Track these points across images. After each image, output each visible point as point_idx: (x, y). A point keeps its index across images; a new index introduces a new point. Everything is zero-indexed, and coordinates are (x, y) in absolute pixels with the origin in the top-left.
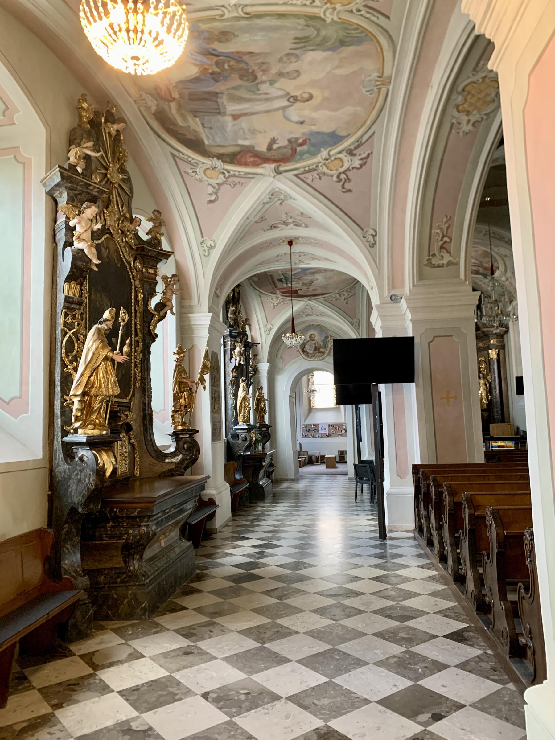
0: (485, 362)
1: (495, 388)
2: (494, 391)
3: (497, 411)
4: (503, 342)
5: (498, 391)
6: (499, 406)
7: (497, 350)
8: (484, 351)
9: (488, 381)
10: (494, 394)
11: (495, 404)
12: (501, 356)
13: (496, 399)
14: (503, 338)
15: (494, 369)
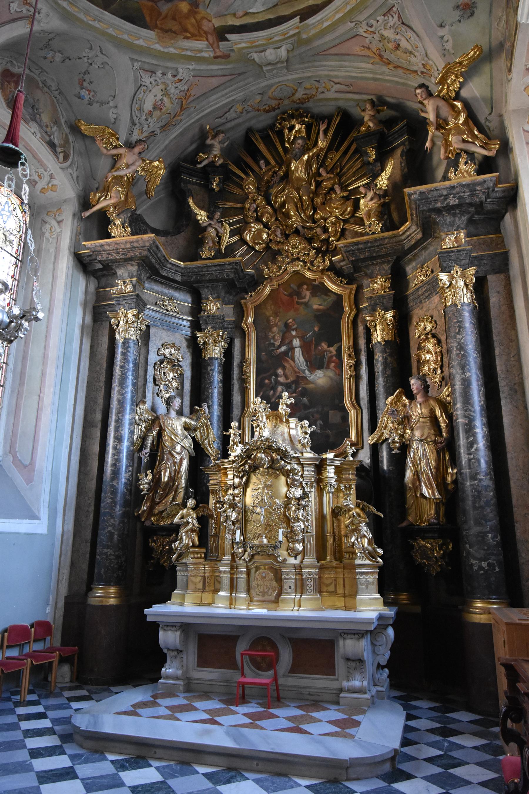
0: (434, 336)
1: (469, 429)
2: (462, 440)
3: (483, 535)
4: (501, 242)
5: (481, 443)
6: (490, 513)
7: (471, 271)
8: (428, 297)
9: (445, 407)
10: (464, 459)
11: (469, 502)
12: (494, 299)
13: (473, 477)
14: (498, 231)
15: (461, 347)
